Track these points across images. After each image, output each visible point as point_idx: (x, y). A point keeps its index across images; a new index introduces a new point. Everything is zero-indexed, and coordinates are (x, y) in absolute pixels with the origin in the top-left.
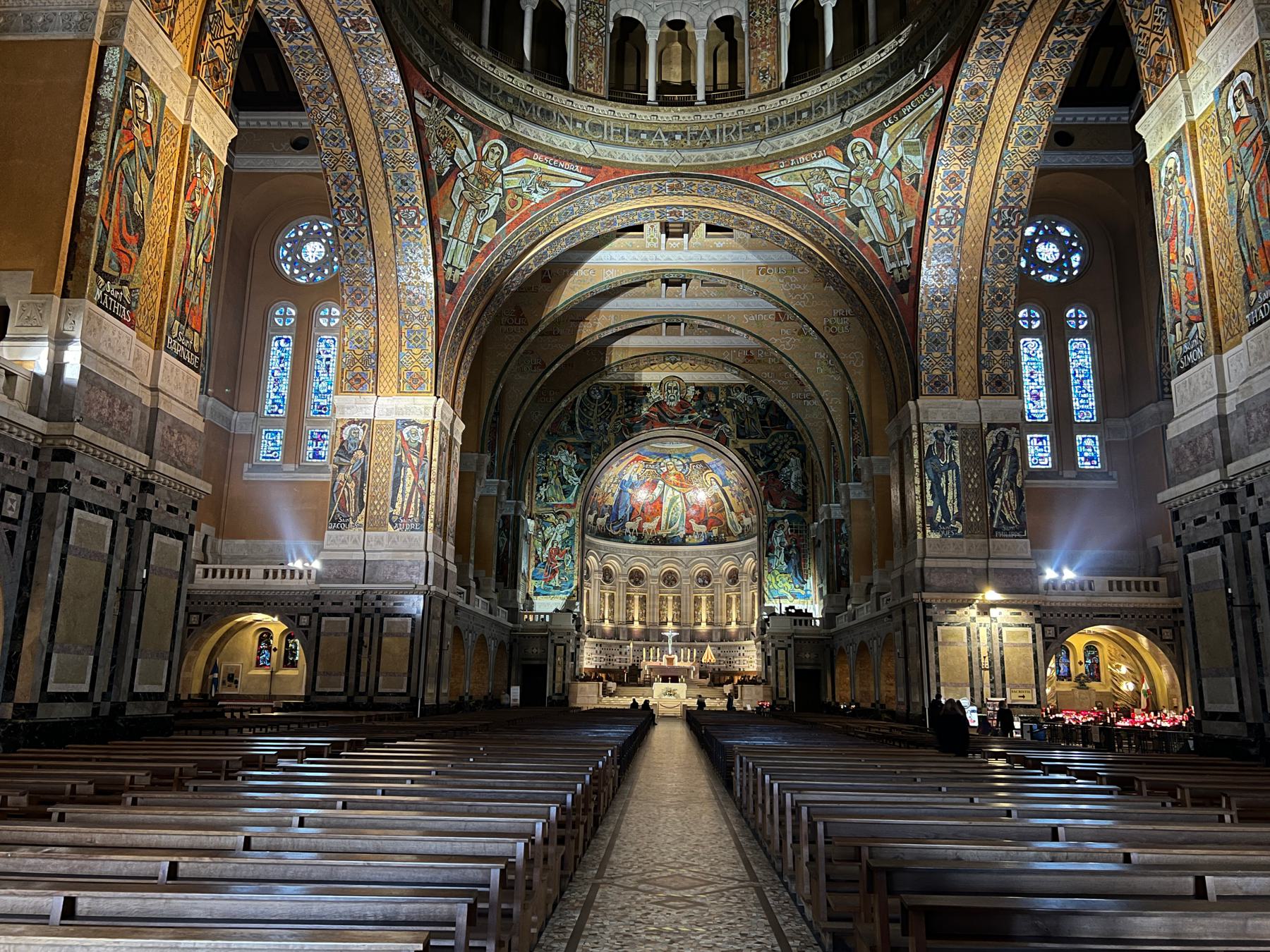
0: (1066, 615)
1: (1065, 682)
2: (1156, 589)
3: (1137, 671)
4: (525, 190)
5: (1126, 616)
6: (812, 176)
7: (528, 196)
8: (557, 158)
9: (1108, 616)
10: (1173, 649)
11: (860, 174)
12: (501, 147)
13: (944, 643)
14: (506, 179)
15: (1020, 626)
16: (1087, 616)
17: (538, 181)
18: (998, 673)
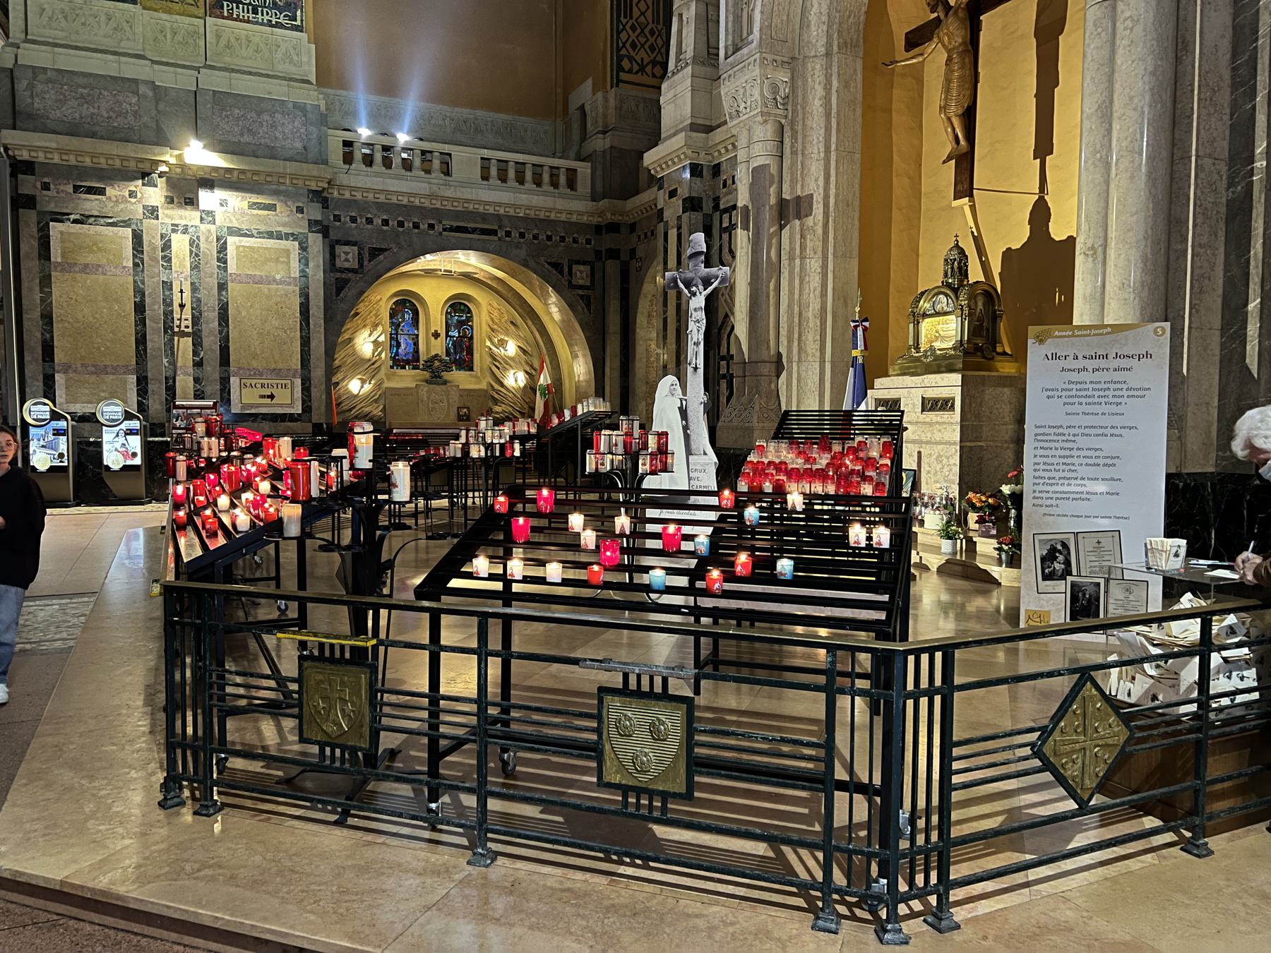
0: (386, 222)
1: (408, 372)
2: (571, 184)
3: (535, 353)
5: (508, 234)
9: (474, 231)
10: (588, 306)
13: (68, 266)
15: (270, 235)
16: (431, 226)
18: (211, 343)
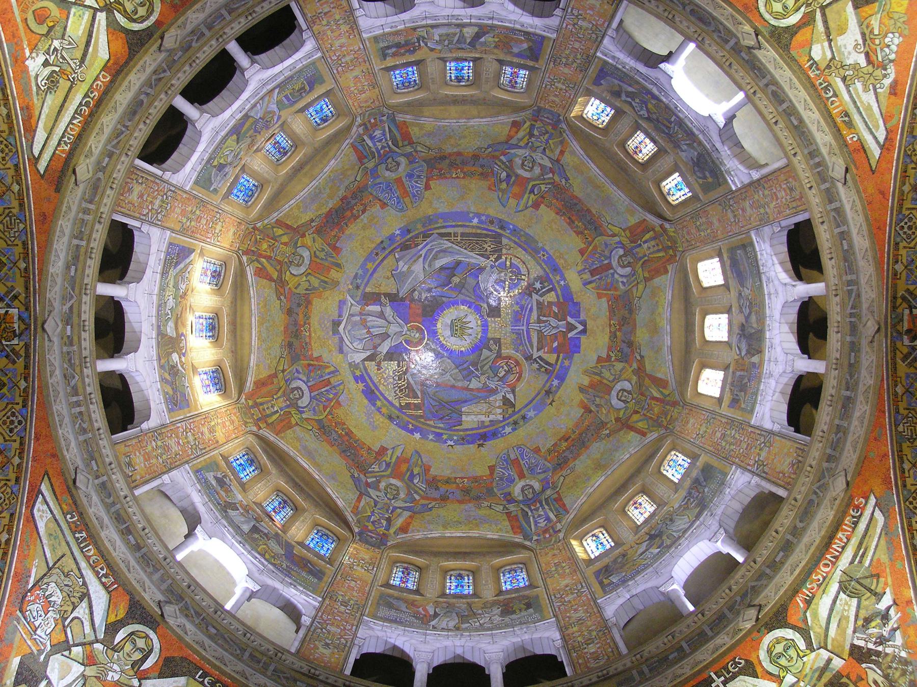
4: (56, 43)
6: (67, 575)
7: (44, 45)
8: (91, 114)
11: (102, 658)
12: (143, 19)
14: (87, 15)
17: (62, 71)
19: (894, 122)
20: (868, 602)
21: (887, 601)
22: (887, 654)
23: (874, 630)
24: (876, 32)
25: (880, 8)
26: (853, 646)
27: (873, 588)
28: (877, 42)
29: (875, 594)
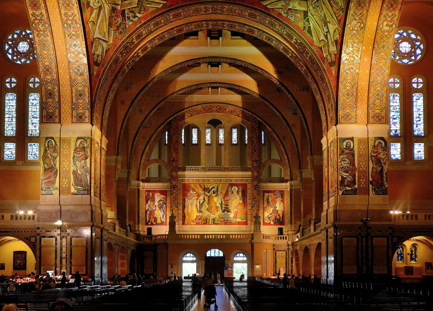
19: (271, 11)
20: (137, 10)
21: (139, 15)
22: (126, 21)
23: (131, 15)
24: (296, 15)
25: (302, 19)
26: (125, 10)
27: (142, 10)
28: (294, 14)
29: (140, 11)
